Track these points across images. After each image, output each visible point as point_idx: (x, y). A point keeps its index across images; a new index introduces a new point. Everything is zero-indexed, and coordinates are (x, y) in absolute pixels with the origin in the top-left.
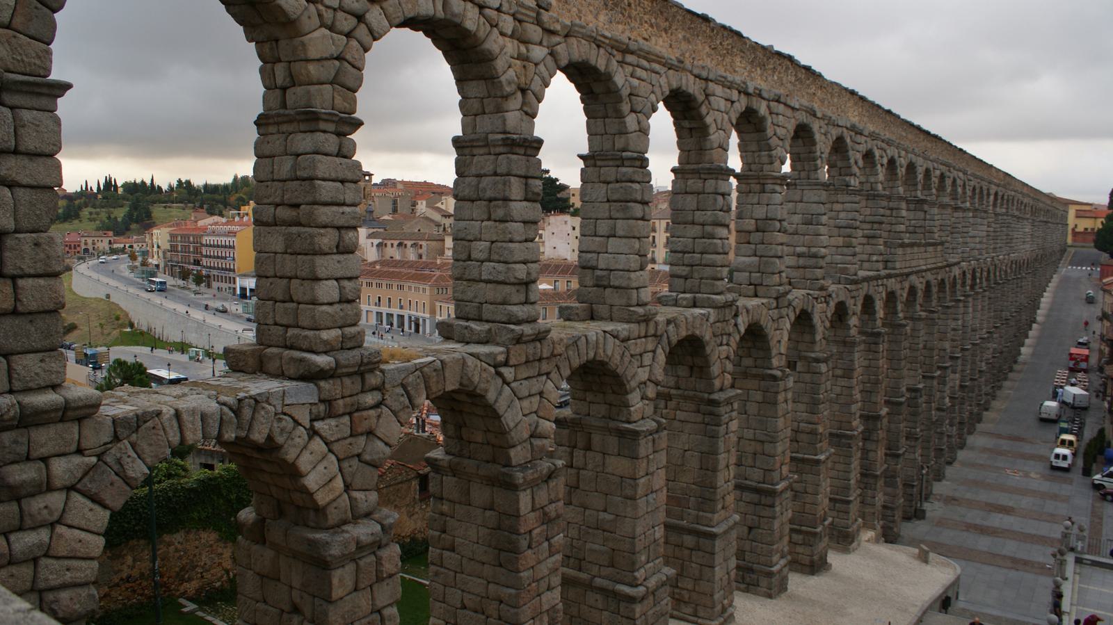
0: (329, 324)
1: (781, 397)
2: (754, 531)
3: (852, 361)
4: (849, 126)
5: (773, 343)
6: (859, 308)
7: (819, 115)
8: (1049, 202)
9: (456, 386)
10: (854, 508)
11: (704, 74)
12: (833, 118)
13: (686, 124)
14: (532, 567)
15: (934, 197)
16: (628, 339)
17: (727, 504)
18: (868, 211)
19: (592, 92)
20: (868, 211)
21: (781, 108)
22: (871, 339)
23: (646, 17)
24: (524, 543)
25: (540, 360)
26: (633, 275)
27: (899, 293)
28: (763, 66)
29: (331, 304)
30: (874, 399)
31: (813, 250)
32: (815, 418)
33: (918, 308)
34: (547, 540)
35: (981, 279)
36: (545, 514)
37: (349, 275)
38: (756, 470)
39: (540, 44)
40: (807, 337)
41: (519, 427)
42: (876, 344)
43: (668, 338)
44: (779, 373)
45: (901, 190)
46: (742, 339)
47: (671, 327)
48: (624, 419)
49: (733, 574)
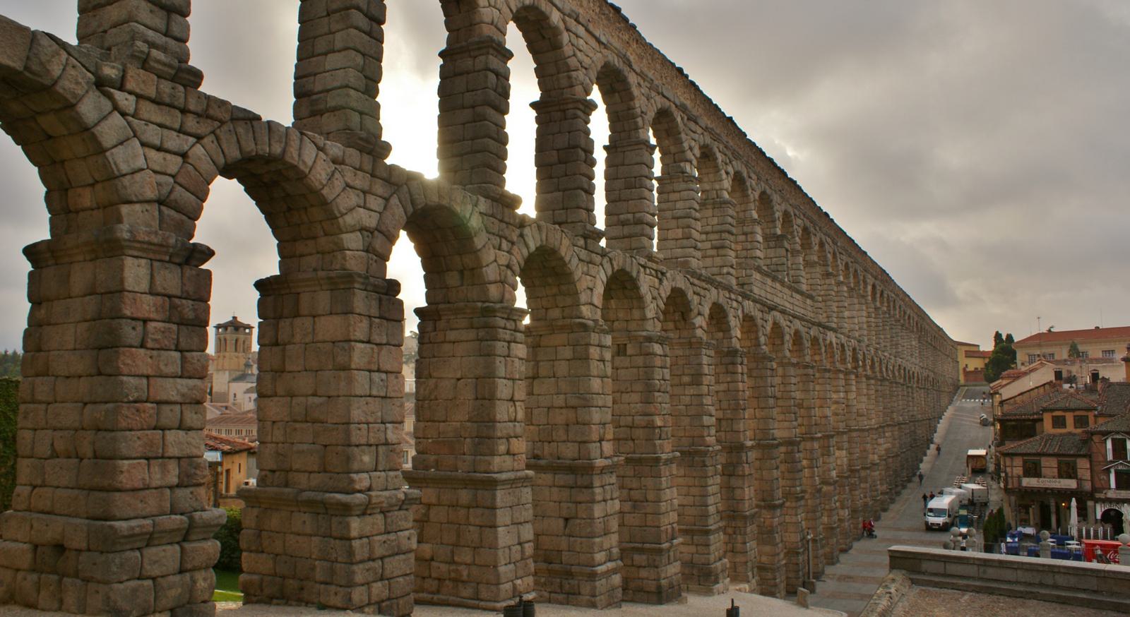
1: (594, 352)
2: (571, 522)
3: (700, 364)
4: (678, 104)
5: (583, 283)
6: (707, 311)
7: (635, 67)
8: (935, 329)
10: (717, 541)
12: (656, 82)
14: (148, 377)
16: (343, 163)
17: (514, 449)
18: (715, 221)
20: (715, 221)
21: (581, 31)
22: (728, 360)
24: (131, 333)
27: (759, 322)
30: (735, 427)
31: (638, 215)
32: (651, 409)
33: (788, 354)
35: (864, 361)
38: (569, 444)
40: (636, 314)
41: (138, 176)
42: (734, 364)
44: (591, 323)
45: (755, 215)
46: (530, 255)
48: (338, 267)
49: (529, 549)
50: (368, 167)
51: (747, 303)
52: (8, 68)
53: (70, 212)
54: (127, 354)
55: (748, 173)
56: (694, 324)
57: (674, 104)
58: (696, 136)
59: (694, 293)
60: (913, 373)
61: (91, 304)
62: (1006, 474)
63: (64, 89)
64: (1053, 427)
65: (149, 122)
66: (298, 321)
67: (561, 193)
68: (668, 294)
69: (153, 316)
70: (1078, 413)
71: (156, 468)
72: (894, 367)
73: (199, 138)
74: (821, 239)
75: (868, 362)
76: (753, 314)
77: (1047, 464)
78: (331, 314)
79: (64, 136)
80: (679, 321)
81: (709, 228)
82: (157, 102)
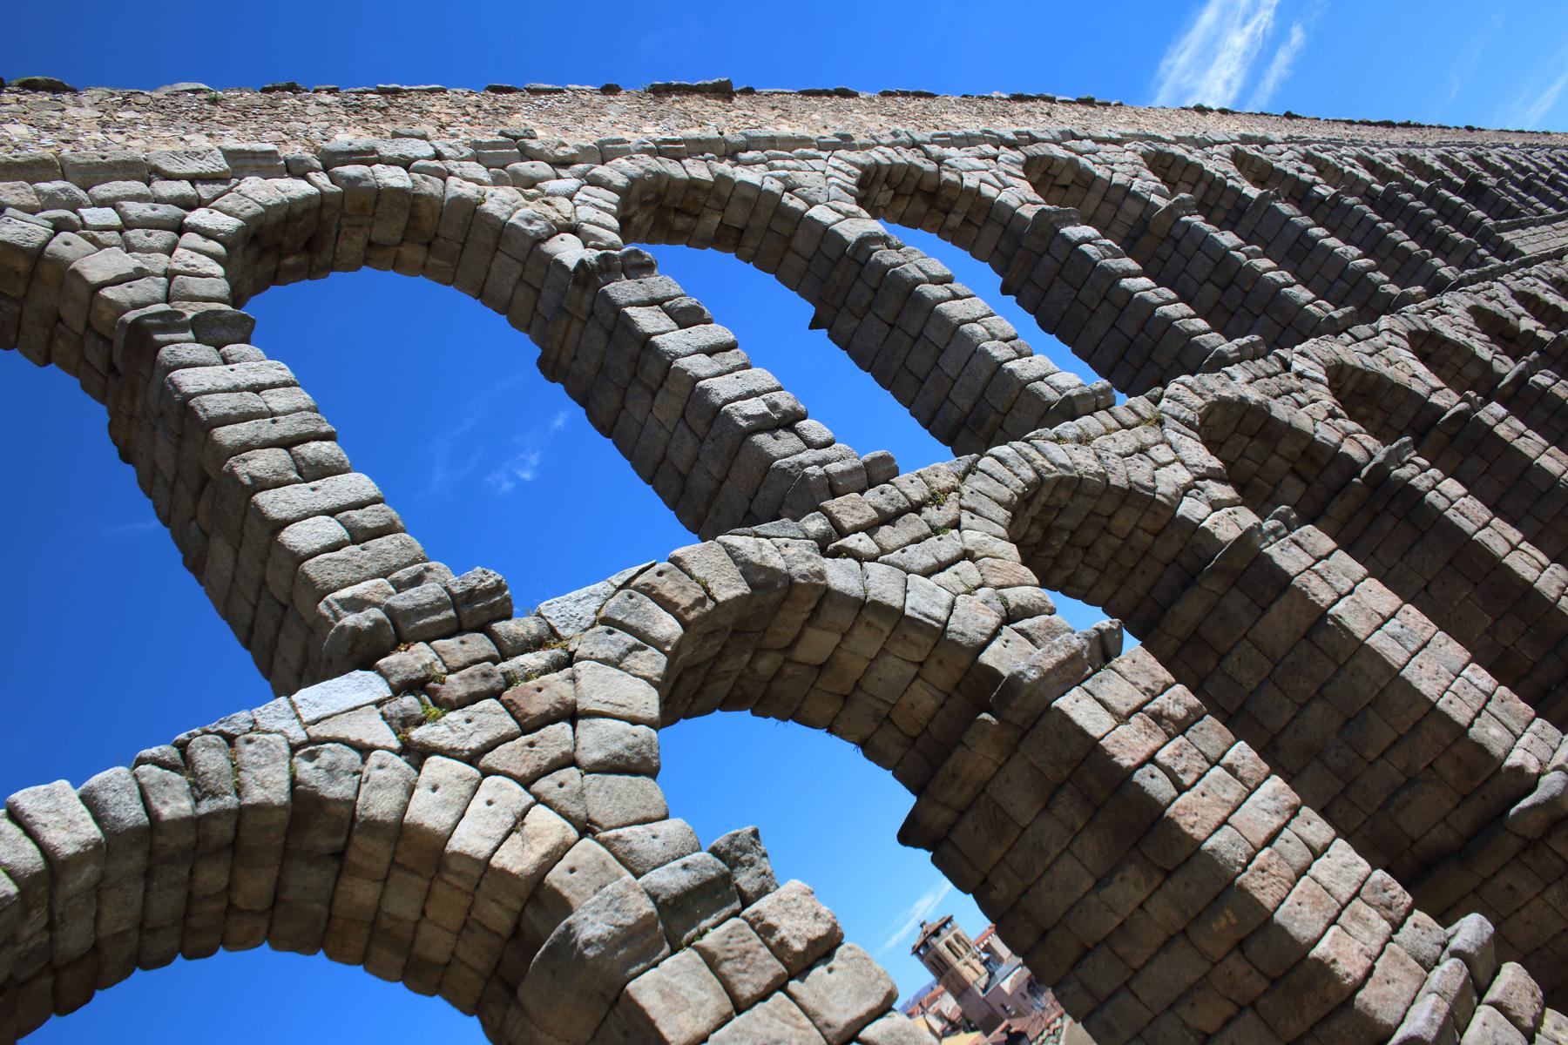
0: (349, 576)
1: (1501, 430)
6: (1520, 309)
9: (742, 588)
11: (904, 138)
12: (1197, 136)
13: (955, 220)
14: (1225, 822)
19: (741, 231)
21: (1088, 144)
23: (732, 114)
24: (1159, 786)
25: (917, 508)
26: (1009, 365)
28: (1004, 113)
29: (336, 547)
34: (1214, 763)
36: (1158, 717)
37: (352, 499)
39: (559, 177)
43: (1177, 418)
44: (1463, 406)
47: (1164, 402)
50: (1114, 424)
51: (1534, 270)
52: (737, 598)
53: (915, 739)
54: (1181, 811)
58: (1289, 155)
61: (1066, 804)
63: (804, 576)
65: (902, 548)
66: (1230, 663)
67: (1264, 316)
69: (1153, 744)
71: (1355, 927)
73: (956, 524)
78: (1264, 610)
79: (838, 646)
82: (888, 519)
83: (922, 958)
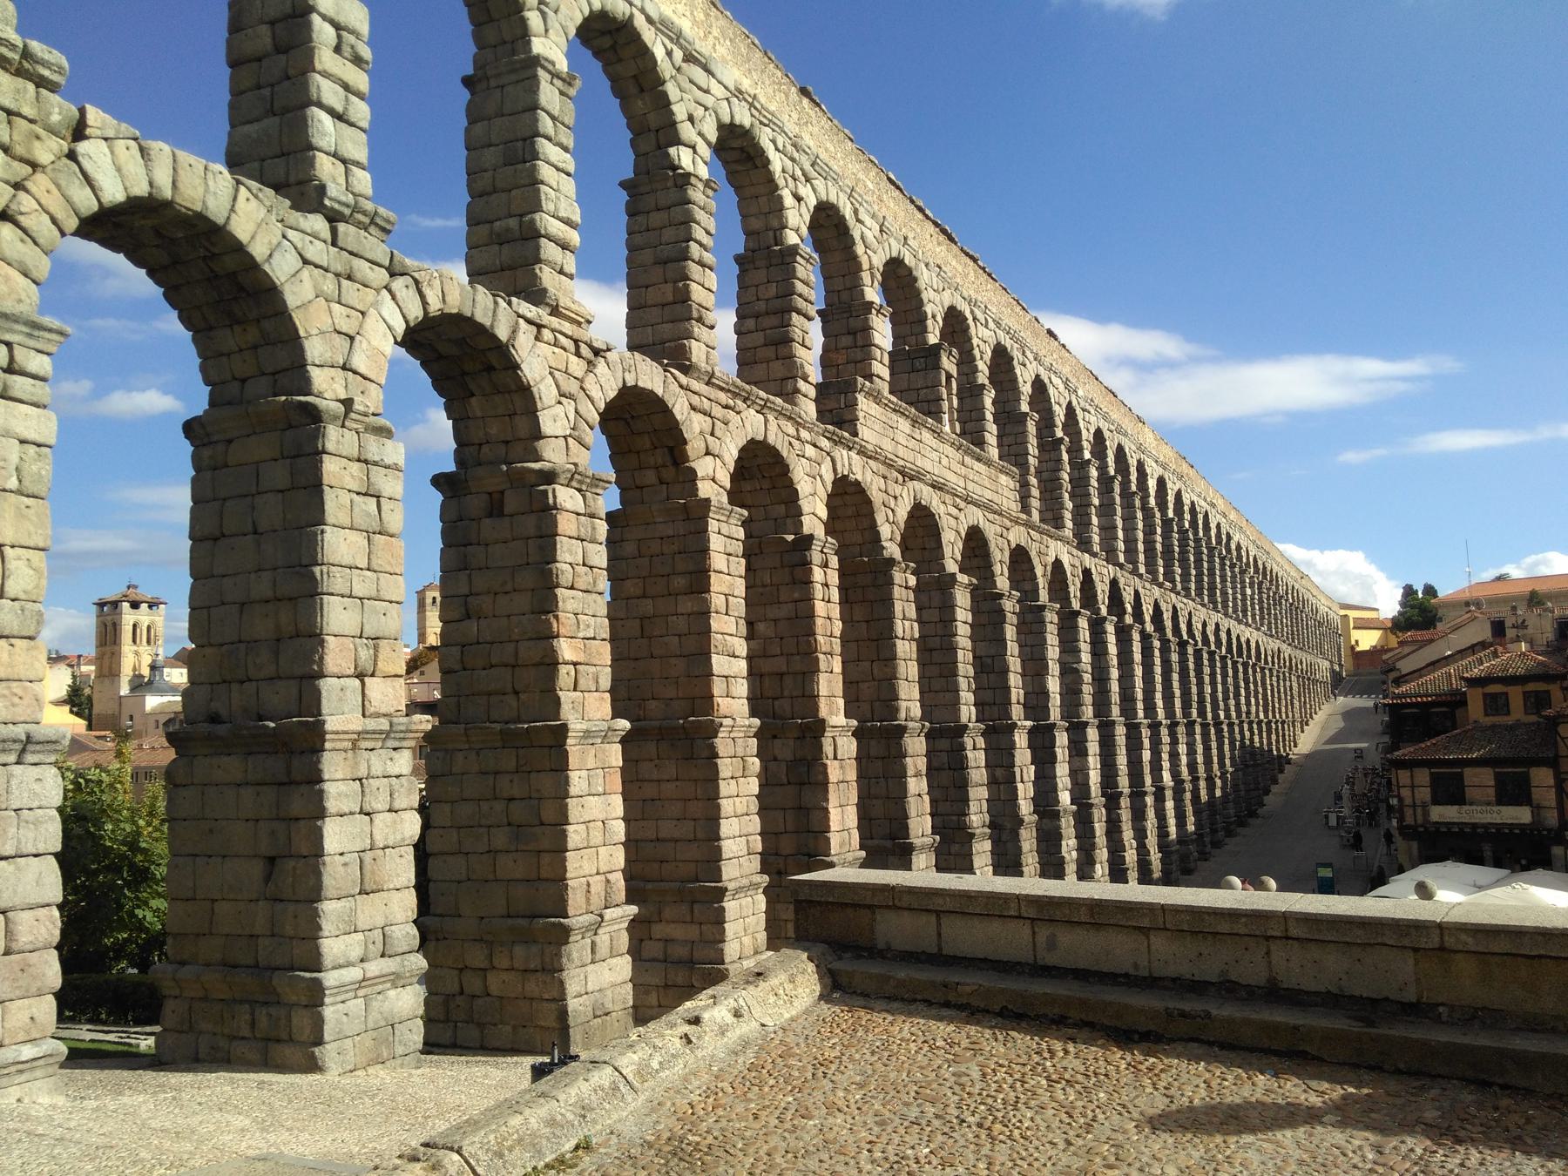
6: (731, 452)
15: (983, 378)
18: (773, 290)
27: (876, 496)
51: (841, 454)
55: (856, 212)
56: (693, 472)
57: (642, 11)
58: (709, 100)
59: (693, 408)
60: (1248, 641)
62: (1401, 799)
64: (1486, 715)
67: (277, 119)
68: (612, 394)
70: (1531, 687)
72: (1204, 625)
74: (1037, 376)
75: (1147, 611)
76: (859, 478)
77: (1476, 781)
80: (664, 466)
81: (761, 306)
83: (100, 614)
